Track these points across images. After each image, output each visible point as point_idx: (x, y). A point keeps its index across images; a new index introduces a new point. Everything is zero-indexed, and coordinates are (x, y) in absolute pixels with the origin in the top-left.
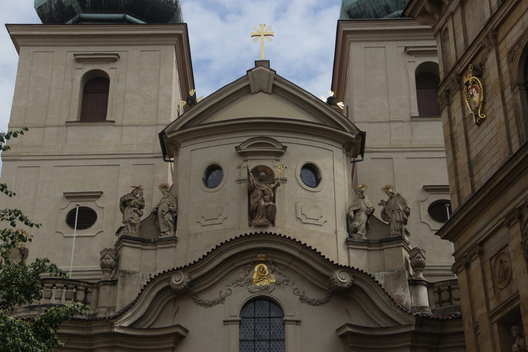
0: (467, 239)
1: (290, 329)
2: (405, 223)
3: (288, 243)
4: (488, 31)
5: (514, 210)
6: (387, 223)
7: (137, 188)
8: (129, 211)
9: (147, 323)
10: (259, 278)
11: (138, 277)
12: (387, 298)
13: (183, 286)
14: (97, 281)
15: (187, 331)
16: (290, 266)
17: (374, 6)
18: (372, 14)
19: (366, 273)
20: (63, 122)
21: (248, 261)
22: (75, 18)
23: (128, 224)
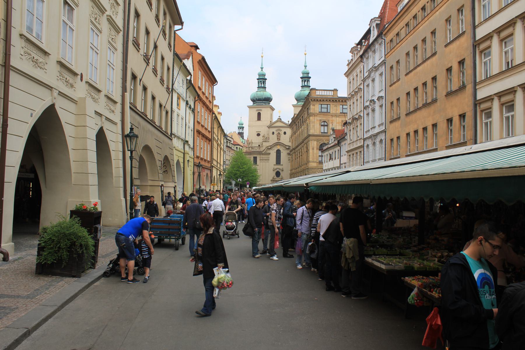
1: (281, 153)
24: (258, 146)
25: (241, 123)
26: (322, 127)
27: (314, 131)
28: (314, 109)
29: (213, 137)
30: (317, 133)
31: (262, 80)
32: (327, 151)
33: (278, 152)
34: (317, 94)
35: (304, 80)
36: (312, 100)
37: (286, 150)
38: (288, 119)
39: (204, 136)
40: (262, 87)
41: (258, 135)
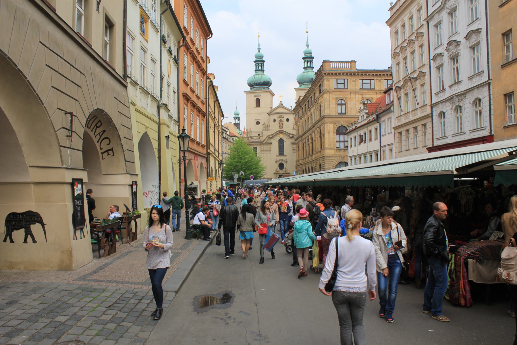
1: (284, 143)
24: (258, 135)
25: (236, 112)
26: (339, 107)
27: (329, 111)
28: (329, 85)
29: (209, 111)
30: (333, 113)
31: (260, 62)
32: (355, 132)
33: (281, 141)
34: (331, 67)
35: (306, 61)
36: (325, 74)
38: (291, 103)
39: (194, 105)
40: (260, 70)
41: (258, 123)
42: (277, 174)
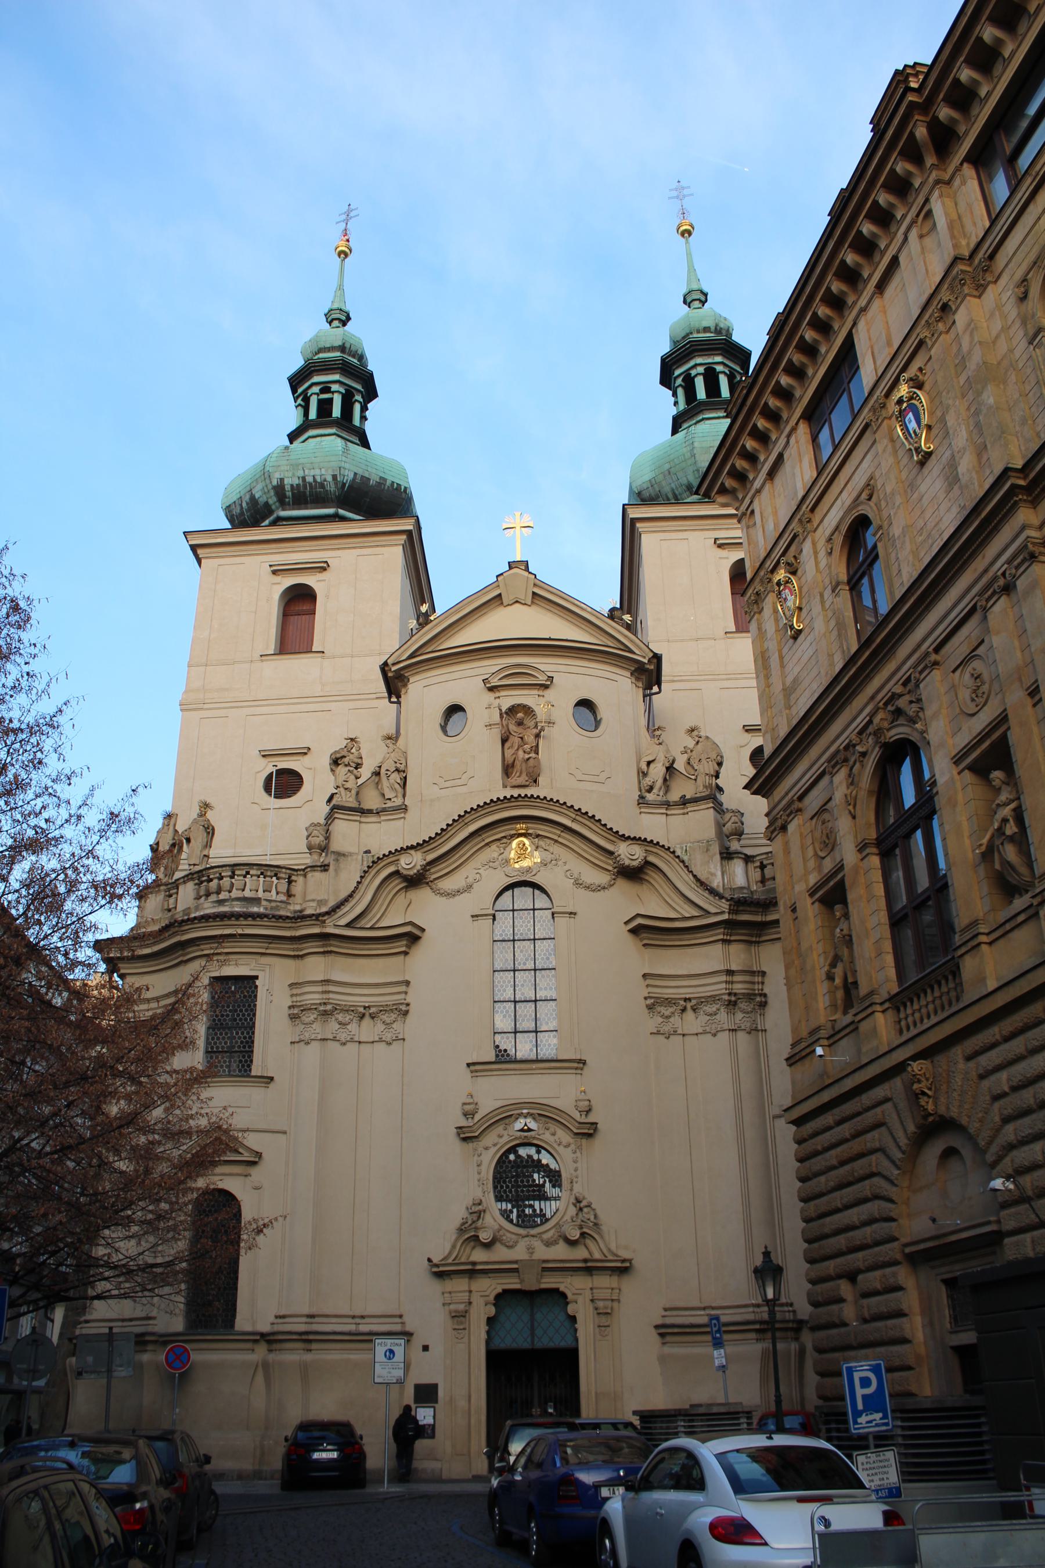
0: (783, 793)
2: (717, 777)
3: (557, 809)
4: (801, 513)
5: (837, 751)
6: (693, 777)
7: (352, 740)
8: (342, 770)
9: (370, 920)
10: (519, 857)
11: (356, 859)
12: (691, 876)
13: (415, 871)
14: (303, 867)
15: (423, 930)
16: (560, 840)
17: (673, 485)
18: (670, 496)
19: (663, 846)
20: (257, 656)
21: (503, 835)
22: (272, 518)
23: (342, 789)
35: (701, 369)
37: (612, 889)
42: (473, 1272)
